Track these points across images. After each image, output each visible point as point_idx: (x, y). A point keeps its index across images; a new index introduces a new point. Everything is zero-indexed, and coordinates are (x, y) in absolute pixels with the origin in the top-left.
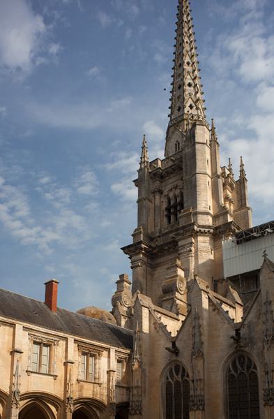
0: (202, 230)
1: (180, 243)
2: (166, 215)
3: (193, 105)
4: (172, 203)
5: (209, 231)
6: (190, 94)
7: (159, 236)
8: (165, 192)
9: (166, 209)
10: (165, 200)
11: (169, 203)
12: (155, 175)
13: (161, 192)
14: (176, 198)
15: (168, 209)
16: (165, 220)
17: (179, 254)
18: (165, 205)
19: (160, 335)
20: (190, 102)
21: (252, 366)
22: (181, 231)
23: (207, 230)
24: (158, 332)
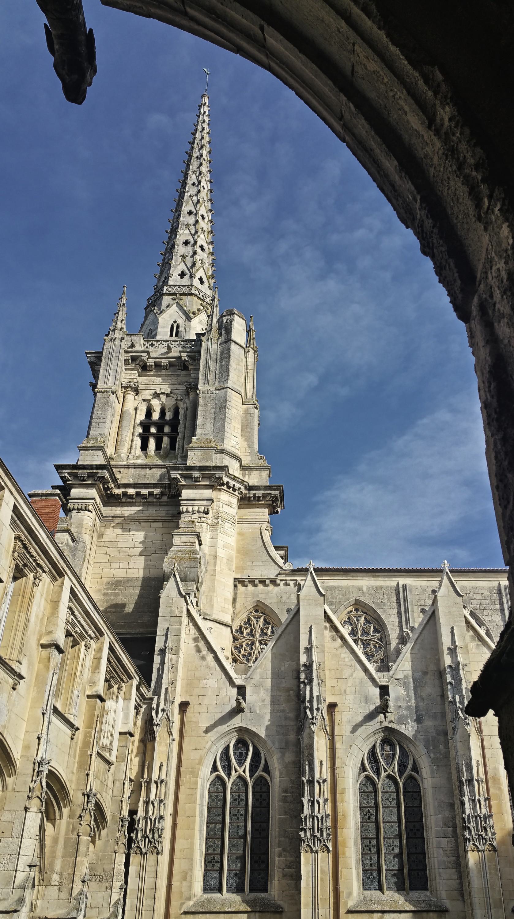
0: (232, 483)
1: (186, 494)
2: (140, 435)
3: (187, 272)
4: (156, 416)
5: (239, 488)
6: (183, 257)
7: (127, 467)
8: (146, 394)
9: (142, 424)
10: (143, 409)
11: (149, 414)
12: (134, 359)
13: (137, 391)
14: (163, 412)
15: (146, 426)
16: (138, 442)
17: (183, 512)
18: (141, 416)
19: (208, 666)
20: (182, 267)
21: (410, 766)
22: (196, 474)
23: (237, 485)
24: (203, 658)
